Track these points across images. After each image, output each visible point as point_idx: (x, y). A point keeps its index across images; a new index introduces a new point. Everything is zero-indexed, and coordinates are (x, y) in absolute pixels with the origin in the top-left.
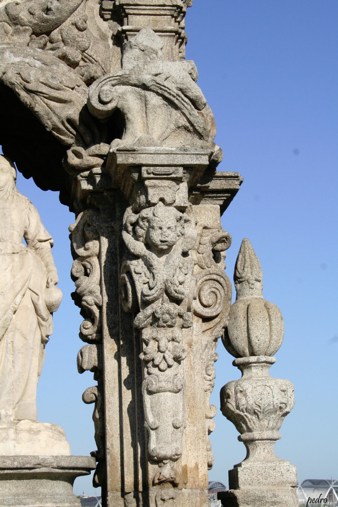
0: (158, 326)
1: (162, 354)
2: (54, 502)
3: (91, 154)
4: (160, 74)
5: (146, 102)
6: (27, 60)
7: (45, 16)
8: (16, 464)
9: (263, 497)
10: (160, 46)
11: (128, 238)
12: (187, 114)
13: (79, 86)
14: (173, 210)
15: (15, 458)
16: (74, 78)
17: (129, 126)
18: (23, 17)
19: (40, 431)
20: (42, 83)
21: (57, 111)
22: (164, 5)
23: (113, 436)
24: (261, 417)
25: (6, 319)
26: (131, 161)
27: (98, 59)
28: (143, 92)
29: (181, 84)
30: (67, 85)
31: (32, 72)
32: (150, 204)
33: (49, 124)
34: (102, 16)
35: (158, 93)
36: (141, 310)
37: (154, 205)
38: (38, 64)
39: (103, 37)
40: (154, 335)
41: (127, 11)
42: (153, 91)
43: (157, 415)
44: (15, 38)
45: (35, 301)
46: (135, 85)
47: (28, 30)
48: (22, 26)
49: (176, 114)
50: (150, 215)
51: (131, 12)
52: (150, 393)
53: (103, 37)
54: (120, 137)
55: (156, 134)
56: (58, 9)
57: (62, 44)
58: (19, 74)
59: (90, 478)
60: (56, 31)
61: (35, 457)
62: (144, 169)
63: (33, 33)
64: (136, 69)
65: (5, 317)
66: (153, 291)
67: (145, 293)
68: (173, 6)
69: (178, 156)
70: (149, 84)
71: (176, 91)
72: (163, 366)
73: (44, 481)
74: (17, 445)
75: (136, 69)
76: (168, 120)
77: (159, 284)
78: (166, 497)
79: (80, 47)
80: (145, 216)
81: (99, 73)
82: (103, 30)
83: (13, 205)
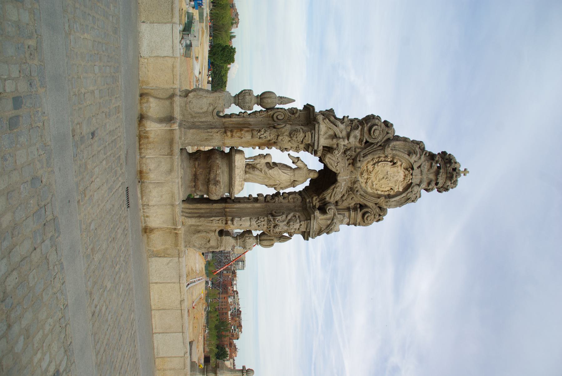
0: (268, 222)
5: (328, 219)
6: (343, 188)
8: (233, 184)
11: (292, 214)
12: (325, 231)
17: (322, 215)
21: (328, 196)
26: (312, 218)
28: (331, 219)
31: (339, 189)
32: (300, 222)
34: (355, 204)
35: (331, 223)
37: (300, 223)
38: (341, 190)
39: (349, 204)
40: (265, 220)
43: (244, 221)
44: (350, 182)
45: (277, 185)
46: (333, 217)
49: (324, 227)
50: (297, 222)
51: (356, 213)
52: (250, 219)
53: (349, 204)
55: (320, 222)
58: (339, 186)
61: (235, 188)
62: (310, 221)
63: (351, 188)
66: (277, 222)
70: (333, 221)
72: (257, 222)
73: (229, 189)
83: (304, 179)
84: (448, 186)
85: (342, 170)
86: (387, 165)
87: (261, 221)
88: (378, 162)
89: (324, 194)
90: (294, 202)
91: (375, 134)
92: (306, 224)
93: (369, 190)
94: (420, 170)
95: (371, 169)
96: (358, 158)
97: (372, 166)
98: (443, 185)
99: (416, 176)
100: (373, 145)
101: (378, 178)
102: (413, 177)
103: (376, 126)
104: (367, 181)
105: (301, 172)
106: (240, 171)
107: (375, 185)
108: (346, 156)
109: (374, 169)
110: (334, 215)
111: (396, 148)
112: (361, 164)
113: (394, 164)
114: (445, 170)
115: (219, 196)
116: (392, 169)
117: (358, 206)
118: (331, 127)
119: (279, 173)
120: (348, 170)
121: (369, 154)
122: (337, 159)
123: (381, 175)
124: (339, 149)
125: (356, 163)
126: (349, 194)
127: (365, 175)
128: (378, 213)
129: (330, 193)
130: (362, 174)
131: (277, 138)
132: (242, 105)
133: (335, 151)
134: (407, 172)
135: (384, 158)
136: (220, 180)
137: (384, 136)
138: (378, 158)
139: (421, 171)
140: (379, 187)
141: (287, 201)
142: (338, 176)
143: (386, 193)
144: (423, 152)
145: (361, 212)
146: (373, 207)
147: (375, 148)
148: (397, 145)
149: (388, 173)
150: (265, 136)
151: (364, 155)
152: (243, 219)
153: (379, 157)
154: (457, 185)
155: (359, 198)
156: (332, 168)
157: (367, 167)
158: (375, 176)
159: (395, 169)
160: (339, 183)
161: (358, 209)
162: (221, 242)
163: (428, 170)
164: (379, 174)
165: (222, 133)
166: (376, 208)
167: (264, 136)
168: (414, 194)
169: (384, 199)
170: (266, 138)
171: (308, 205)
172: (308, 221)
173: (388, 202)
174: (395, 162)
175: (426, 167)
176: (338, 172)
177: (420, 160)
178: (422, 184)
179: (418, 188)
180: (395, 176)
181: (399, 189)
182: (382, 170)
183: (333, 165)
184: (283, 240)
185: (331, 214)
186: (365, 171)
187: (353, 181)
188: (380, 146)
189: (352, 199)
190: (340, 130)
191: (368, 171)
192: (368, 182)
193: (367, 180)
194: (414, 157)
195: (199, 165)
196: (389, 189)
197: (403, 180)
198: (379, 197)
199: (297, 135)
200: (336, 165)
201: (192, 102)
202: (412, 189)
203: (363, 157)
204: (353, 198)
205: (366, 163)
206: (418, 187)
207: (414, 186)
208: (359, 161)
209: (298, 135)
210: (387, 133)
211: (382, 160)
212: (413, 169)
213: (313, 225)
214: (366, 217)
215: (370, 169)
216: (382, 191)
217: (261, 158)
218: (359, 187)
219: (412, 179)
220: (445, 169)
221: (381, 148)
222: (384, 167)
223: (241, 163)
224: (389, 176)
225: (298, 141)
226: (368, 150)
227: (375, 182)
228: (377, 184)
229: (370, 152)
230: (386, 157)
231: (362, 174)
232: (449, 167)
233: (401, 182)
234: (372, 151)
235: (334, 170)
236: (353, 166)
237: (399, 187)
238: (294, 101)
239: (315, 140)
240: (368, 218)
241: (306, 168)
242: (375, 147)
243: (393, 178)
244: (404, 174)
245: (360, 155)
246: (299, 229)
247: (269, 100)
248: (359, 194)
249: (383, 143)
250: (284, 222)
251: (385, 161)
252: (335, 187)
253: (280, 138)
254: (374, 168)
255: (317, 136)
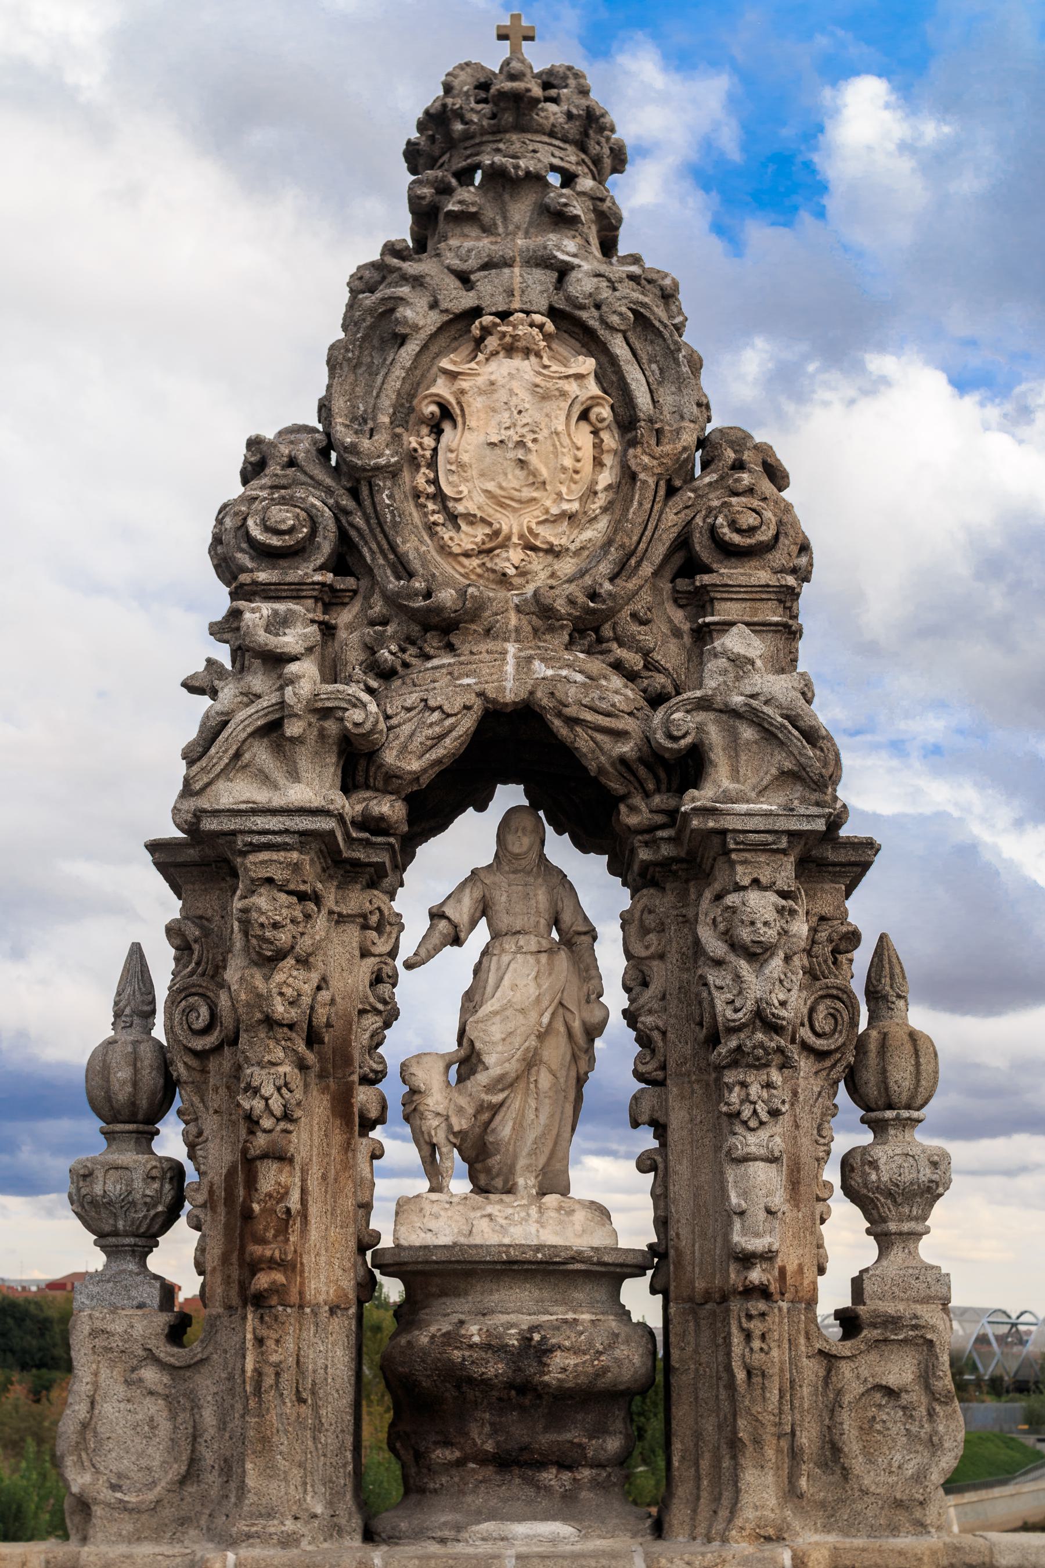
1: (752, 1106)
2: (593, 1313)
3: (654, 809)
4: (758, 694)
6: (564, 672)
7: (592, 605)
9: (900, 1318)
10: (758, 653)
12: (796, 752)
13: (638, 710)
14: (773, 897)
15: (538, 1248)
16: (632, 697)
17: (711, 770)
18: (559, 608)
19: (573, 1211)
20: (586, 706)
22: (768, 586)
23: (678, 1221)
24: (899, 1200)
25: (528, 1048)
26: (711, 824)
27: (668, 665)
29: (788, 709)
30: (621, 708)
32: (739, 888)
33: (592, 767)
36: (723, 1041)
38: (579, 678)
41: (712, 594)
42: (747, 719)
43: (745, 1194)
44: (548, 637)
46: (721, 711)
47: (566, 625)
48: (558, 620)
51: (718, 595)
54: (696, 786)
56: (610, 595)
57: (615, 646)
58: (552, 693)
59: (644, 1282)
60: (607, 626)
61: (567, 1248)
64: (721, 688)
65: (527, 1044)
66: (740, 1015)
67: (729, 1017)
68: (782, 586)
69: (781, 818)
71: (780, 719)
72: (753, 1124)
74: (541, 1230)
75: (721, 688)
76: (769, 762)
77: (749, 1003)
78: (754, 1312)
79: (641, 648)
80: (730, 904)
81: (670, 689)
82: (676, 622)
83: (540, 880)
84: (570, 116)
85: (466, 681)
86: (451, 451)
87: (746, 1100)
88: (439, 496)
89: (601, 770)
90: (661, 929)
91: (283, 527)
92: (748, 855)
93: (593, 533)
94: (482, 273)
95: (480, 533)
96: (417, 605)
97: (464, 527)
98: (565, 140)
99: (511, 293)
100: (353, 533)
101: (525, 489)
102: (516, 305)
103: (250, 522)
104: (544, 546)
105: (504, 899)
106: (484, 1223)
107: (565, 506)
108: (406, 665)
109: (479, 514)
110: (704, 704)
111: (365, 411)
112: (449, 582)
113: (446, 413)
114: (485, 139)
115: (617, 1335)
116: (472, 422)
117: (682, 584)
118: (231, 752)
119: (495, 1013)
120: (472, 653)
121: (393, 548)
122: (409, 710)
123: (506, 474)
124: (346, 706)
125: (439, 610)
126: (617, 639)
127: (508, 560)
128: (722, 478)
129: (591, 737)
130: (503, 580)
131: (282, 1025)
132: (141, 1215)
133: (349, 725)
134: (492, 342)
135: (418, 467)
136: (525, 1327)
137: (309, 481)
138: (422, 500)
139: (486, 266)
140: (575, 483)
141: (655, 963)
142: (494, 701)
143: (610, 441)
144: (392, 270)
145: (715, 566)
146: (687, 507)
147: (367, 521)
148: (355, 407)
149: (495, 439)
150: (279, 1089)
151: (404, 574)
152: (734, 1200)
153: (417, 494)
154: (570, 68)
155: (631, 585)
156: (454, 734)
157: (467, 555)
158: (515, 510)
159: (476, 404)
160: (539, 694)
161: (698, 584)
162: (893, 1322)
163: (488, 230)
164: (501, 488)
165: (267, 1318)
166: (693, 491)
167: (276, 1095)
168: (615, 289)
169: (639, 450)
170: (286, 1085)
171: (666, 851)
172: (732, 846)
173: (657, 426)
174: (434, 408)
175: (468, 244)
176: (478, 704)
177: (428, 279)
178: (555, 257)
179: (580, 276)
180: (514, 401)
181: (579, 377)
182: (482, 475)
183: (438, 729)
184: (892, 977)
185: (700, 728)
186: (489, 565)
187: (537, 622)
188: (354, 493)
189: (644, 623)
190: (247, 705)
191: (488, 546)
192: (548, 543)
193: (534, 549)
194: (409, 313)
195: (447, 1443)
196: (585, 428)
197: (533, 358)
198: (629, 476)
199: (262, 925)
200: (436, 716)
201: (120, 1476)
202: (582, 307)
203: (411, 575)
204: (634, 616)
205: (450, 560)
206: (574, 275)
207: (569, 299)
208: (428, 595)
209: (262, 919)
210: (292, 462)
211: (428, 482)
212: (476, 312)
213: (749, 814)
214: (737, 539)
215: (478, 539)
216: (598, 463)
217: (421, 1108)
218: (571, 588)
219: (527, 313)
220: (477, 141)
221: (365, 492)
222: (461, 465)
223: (442, 1213)
224: (511, 432)
225: (300, 916)
226: (378, 555)
227: (548, 503)
228: (559, 494)
229: (386, 546)
230: (412, 459)
231: (504, 575)
232: (465, 122)
233: (545, 367)
234: (380, 537)
235: (467, 724)
236: (458, 629)
237: (567, 377)
238: (136, 953)
239: (282, 827)
240: (745, 527)
241: (482, 875)
242: (359, 520)
243: (520, 412)
244: (502, 354)
245: (398, 594)
246: (784, 895)
247: (119, 1074)
248: (607, 586)
249: (338, 482)
250: (739, 977)
251: (433, 464)
252: (559, 715)
253: (279, 1008)
254: (475, 516)
255: (262, 822)
